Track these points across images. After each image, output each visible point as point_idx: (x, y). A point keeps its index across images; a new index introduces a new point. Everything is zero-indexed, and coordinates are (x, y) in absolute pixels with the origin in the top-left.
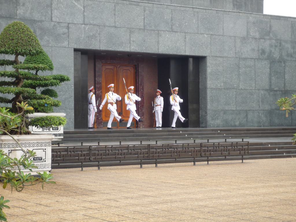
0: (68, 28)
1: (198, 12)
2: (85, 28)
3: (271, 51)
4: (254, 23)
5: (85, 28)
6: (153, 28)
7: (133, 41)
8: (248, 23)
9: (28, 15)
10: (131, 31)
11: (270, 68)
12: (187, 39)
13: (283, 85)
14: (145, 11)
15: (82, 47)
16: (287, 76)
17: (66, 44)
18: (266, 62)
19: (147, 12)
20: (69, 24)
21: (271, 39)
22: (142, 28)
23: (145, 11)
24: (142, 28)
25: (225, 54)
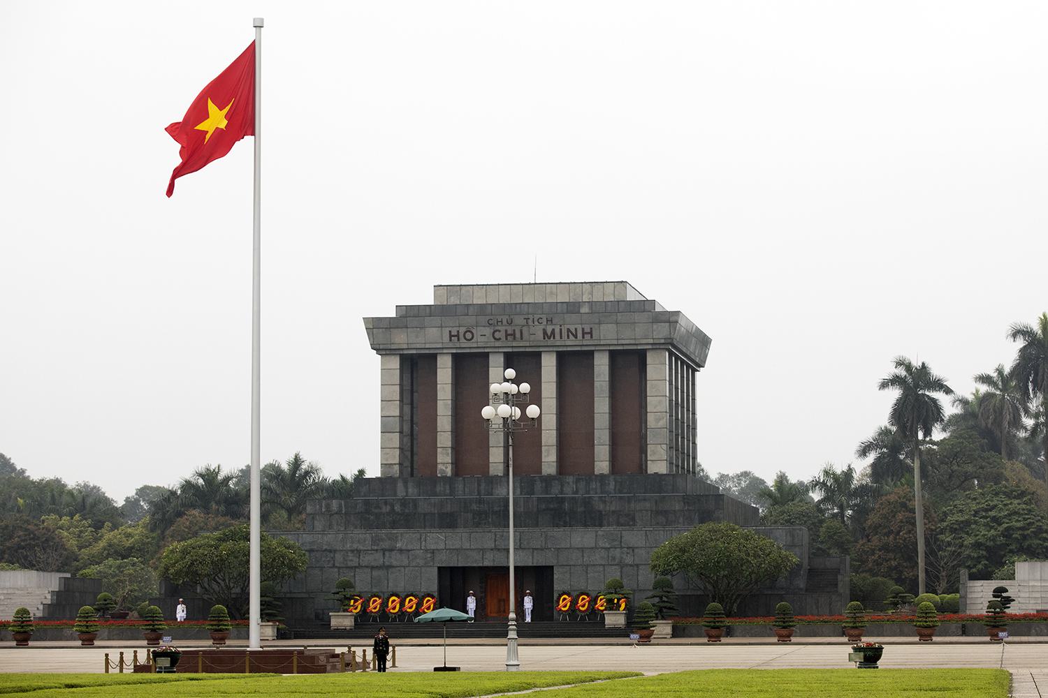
0: (433, 553)
1: (545, 532)
2: (446, 552)
3: (622, 558)
4: (603, 535)
5: (446, 552)
6: (503, 547)
7: (486, 559)
8: (596, 536)
9: (404, 548)
10: (483, 550)
11: (621, 572)
12: (535, 554)
13: (636, 586)
14: (496, 536)
15: (444, 565)
16: (640, 578)
17: (431, 564)
18: (617, 567)
19: (498, 536)
20: (434, 550)
21: (622, 548)
22: (493, 547)
23: (496, 536)
24: (493, 547)
25: (572, 563)
